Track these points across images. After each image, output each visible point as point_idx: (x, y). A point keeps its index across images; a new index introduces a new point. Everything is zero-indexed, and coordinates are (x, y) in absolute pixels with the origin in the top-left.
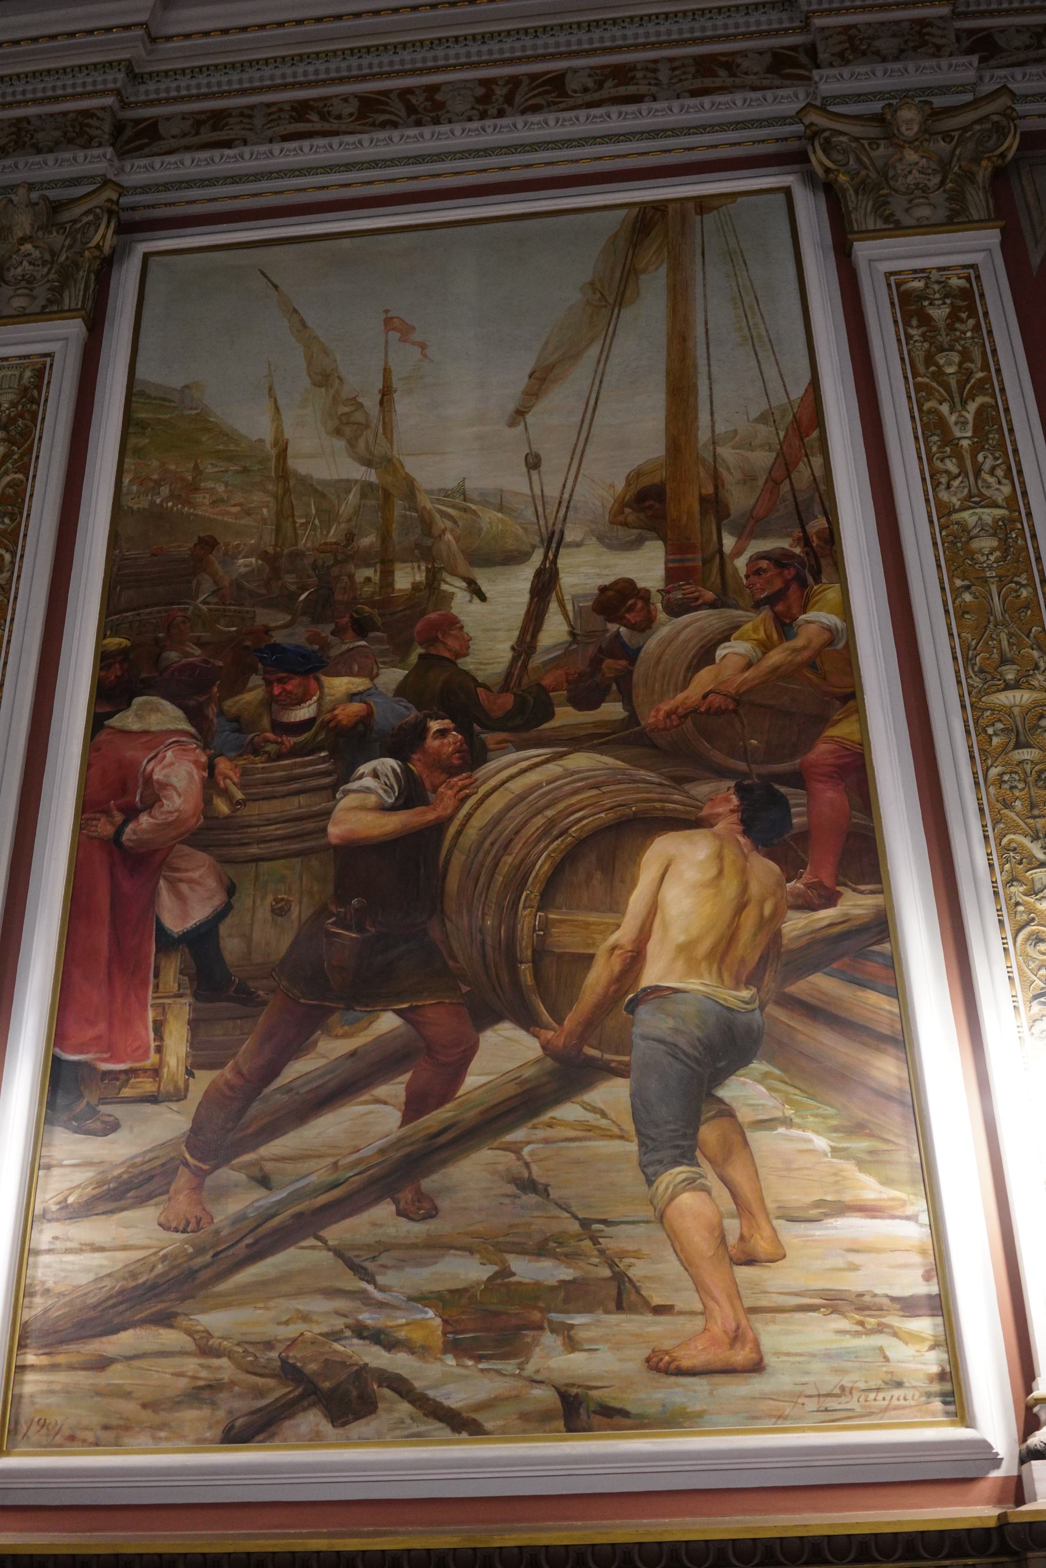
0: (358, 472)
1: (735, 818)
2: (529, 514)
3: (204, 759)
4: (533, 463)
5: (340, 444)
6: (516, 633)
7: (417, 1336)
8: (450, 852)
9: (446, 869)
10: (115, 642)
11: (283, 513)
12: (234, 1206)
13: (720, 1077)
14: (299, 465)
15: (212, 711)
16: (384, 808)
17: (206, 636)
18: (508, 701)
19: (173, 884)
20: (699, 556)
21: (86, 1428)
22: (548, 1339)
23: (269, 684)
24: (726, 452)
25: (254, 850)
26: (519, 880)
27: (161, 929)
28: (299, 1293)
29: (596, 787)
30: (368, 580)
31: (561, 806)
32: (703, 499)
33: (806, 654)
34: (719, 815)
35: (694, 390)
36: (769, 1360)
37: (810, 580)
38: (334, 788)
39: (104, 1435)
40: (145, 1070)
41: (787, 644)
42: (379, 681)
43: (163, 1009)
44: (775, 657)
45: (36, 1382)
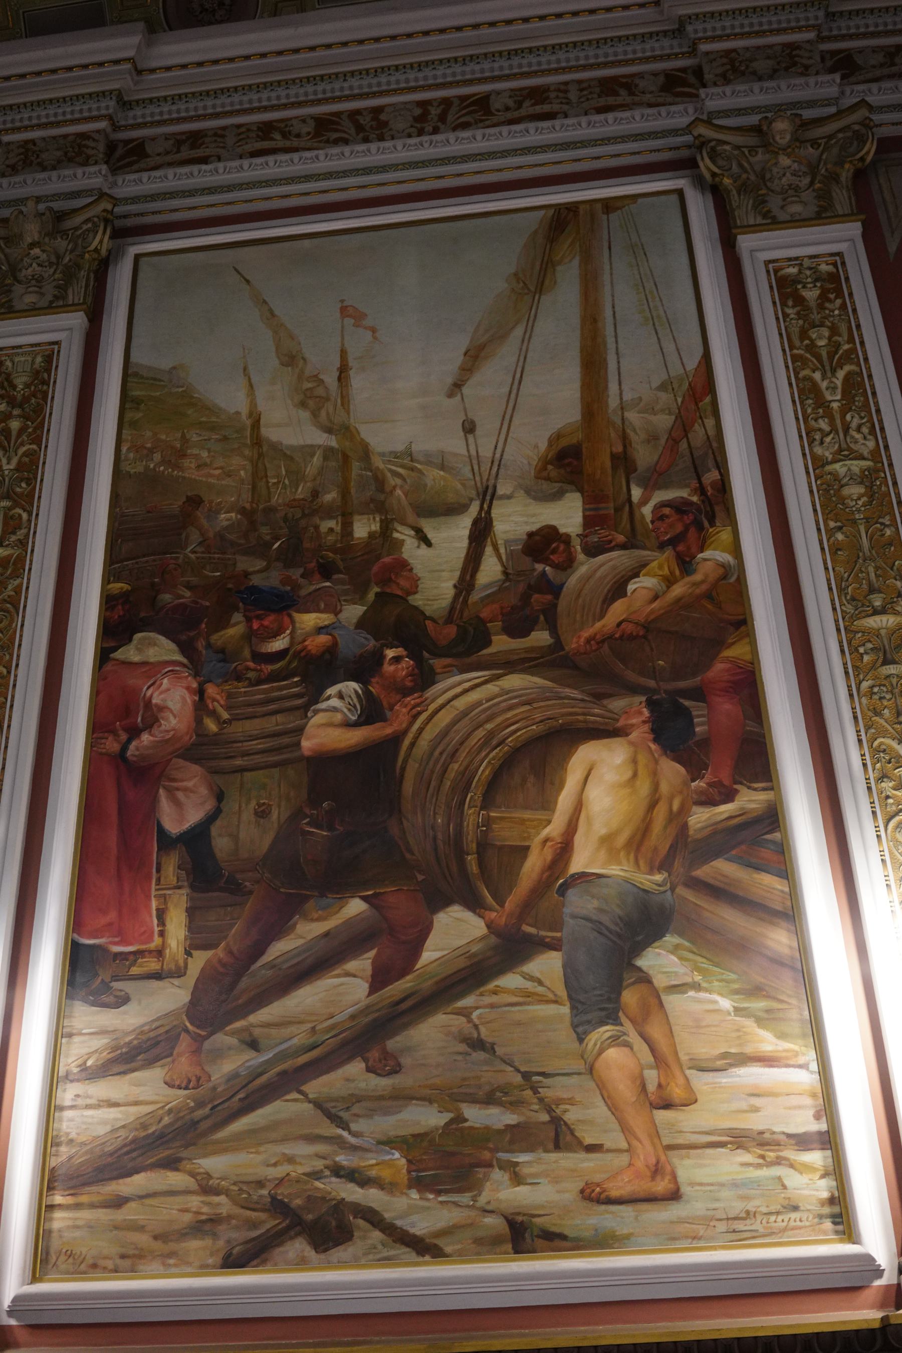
0: (320, 438)
1: (646, 728)
2: (467, 471)
3: (195, 685)
4: (469, 428)
5: (305, 415)
6: (457, 574)
7: (386, 1174)
8: (405, 761)
9: (402, 776)
10: (117, 587)
11: (258, 475)
12: (227, 1066)
13: (638, 949)
14: (271, 433)
15: (201, 644)
16: (348, 725)
17: (194, 580)
18: (452, 631)
19: (170, 792)
20: (611, 505)
21: (106, 1258)
22: (497, 1175)
23: (249, 620)
24: (632, 416)
25: (238, 762)
26: (465, 783)
27: (161, 831)
28: (284, 1139)
29: (528, 703)
30: (331, 530)
31: (499, 720)
32: (614, 457)
33: (704, 587)
34: (633, 725)
35: (604, 363)
36: (685, 1189)
37: (706, 524)
38: (306, 707)
40: (150, 952)
41: (687, 579)
42: (343, 616)
44: (678, 590)
45: (63, 1218)
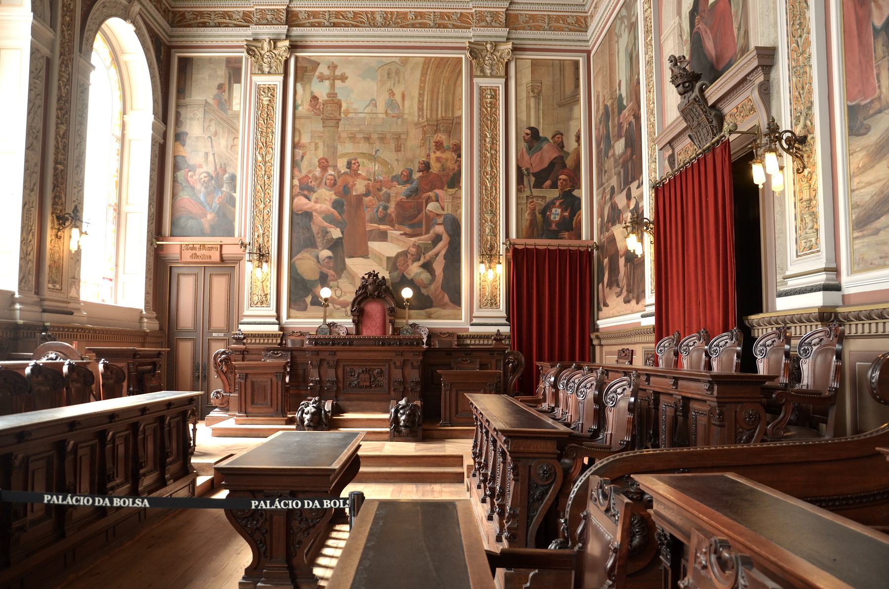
21: (875, 259)
39: (882, 261)
40: (876, 99)
43: (878, 67)
45: (860, 243)
